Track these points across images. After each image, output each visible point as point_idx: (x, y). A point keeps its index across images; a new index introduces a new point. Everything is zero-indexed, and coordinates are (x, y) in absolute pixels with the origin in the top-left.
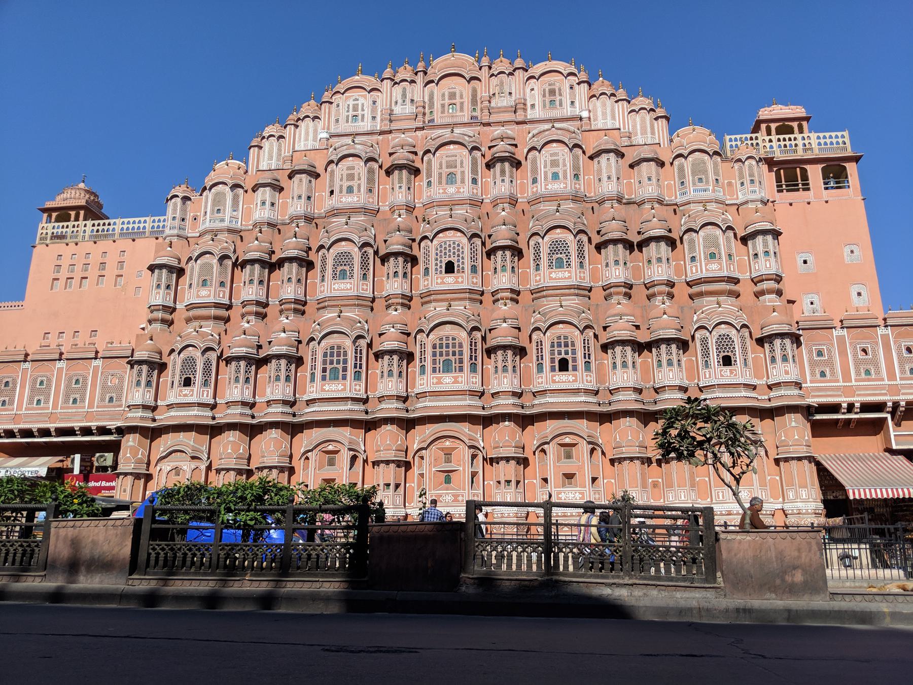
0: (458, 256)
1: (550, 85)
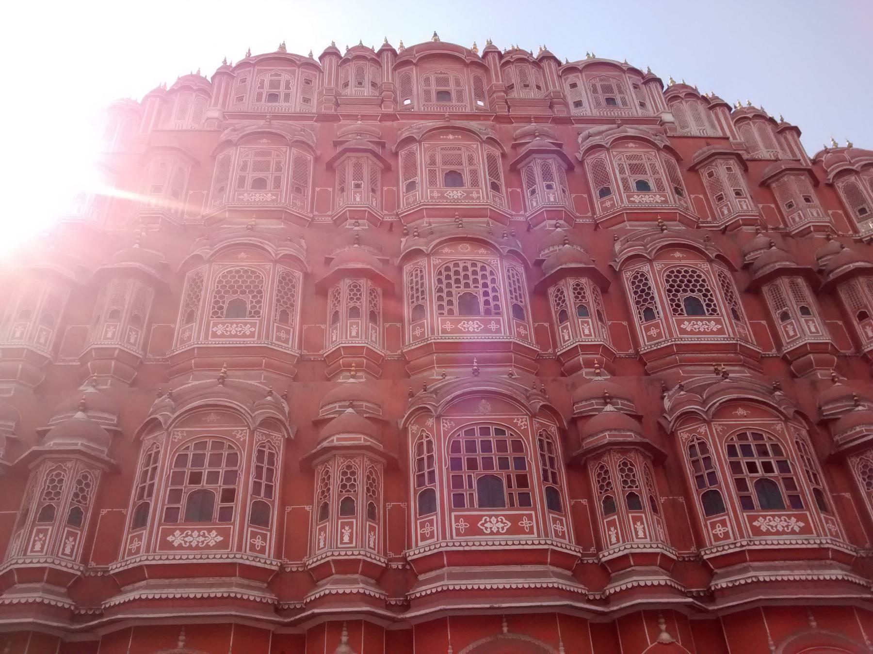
0: (485, 285)
1: (601, 80)
